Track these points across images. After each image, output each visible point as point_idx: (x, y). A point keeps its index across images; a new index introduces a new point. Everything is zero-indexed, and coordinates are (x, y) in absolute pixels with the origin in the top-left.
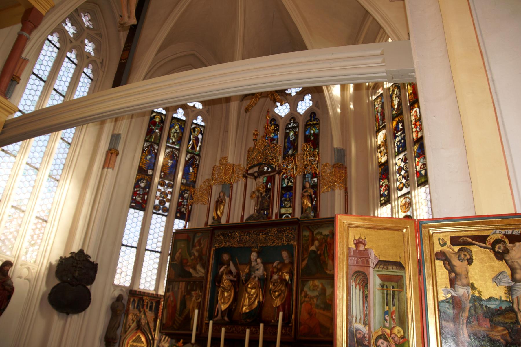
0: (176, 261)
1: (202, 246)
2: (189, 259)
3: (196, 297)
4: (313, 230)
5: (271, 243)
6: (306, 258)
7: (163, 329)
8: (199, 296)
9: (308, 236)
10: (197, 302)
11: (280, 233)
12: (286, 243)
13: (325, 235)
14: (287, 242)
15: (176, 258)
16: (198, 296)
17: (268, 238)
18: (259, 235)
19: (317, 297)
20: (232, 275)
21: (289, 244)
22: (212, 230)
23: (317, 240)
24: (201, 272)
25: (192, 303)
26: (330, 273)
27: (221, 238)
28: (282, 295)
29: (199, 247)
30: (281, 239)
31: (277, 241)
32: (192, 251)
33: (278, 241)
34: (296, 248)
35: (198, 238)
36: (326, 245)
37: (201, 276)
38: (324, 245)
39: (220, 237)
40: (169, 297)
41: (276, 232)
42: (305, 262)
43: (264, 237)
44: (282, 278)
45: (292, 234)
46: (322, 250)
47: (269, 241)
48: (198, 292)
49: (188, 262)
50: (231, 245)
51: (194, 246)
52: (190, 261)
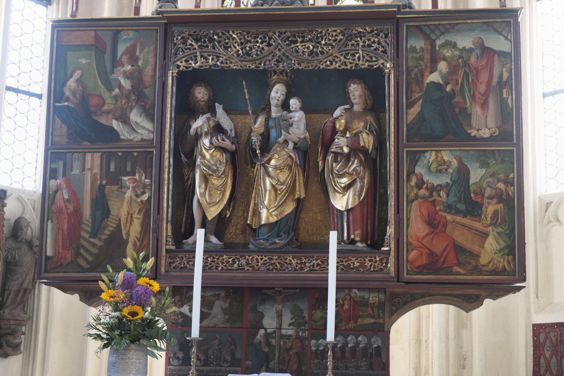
0: (68, 99)
1: (140, 63)
2: (106, 96)
3: (134, 188)
4: (434, 37)
5: (328, 63)
6: (419, 99)
7: (46, 271)
8: (144, 186)
9: (422, 49)
10: (139, 200)
11: (350, 41)
12: (367, 64)
13: (464, 48)
14: (367, 61)
15: (67, 93)
16: (139, 189)
17: (320, 49)
18: (296, 42)
19: (447, 187)
20: (229, 138)
21: (372, 66)
22: (166, 24)
23: (445, 59)
24: (144, 128)
25: (125, 204)
26: (477, 135)
27: (191, 44)
28: (358, 185)
29: (132, 66)
30: (353, 55)
31: (342, 58)
32: (114, 76)
33: (345, 58)
34: (392, 76)
35: (128, 44)
36: (465, 71)
37: (144, 137)
38: (461, 72)
39: (189, 42)
40: (56, 192)
41: (340, 37)
42: (415, 110)
43: (308, 48)
44: (359, 143)
45: (379, 43)
46: (457, 84)
47: (321, 57)
48: (140, 176)
49: (104, 103)
50: (222, 63)
51: (116, 63)
52: (109, 100)
